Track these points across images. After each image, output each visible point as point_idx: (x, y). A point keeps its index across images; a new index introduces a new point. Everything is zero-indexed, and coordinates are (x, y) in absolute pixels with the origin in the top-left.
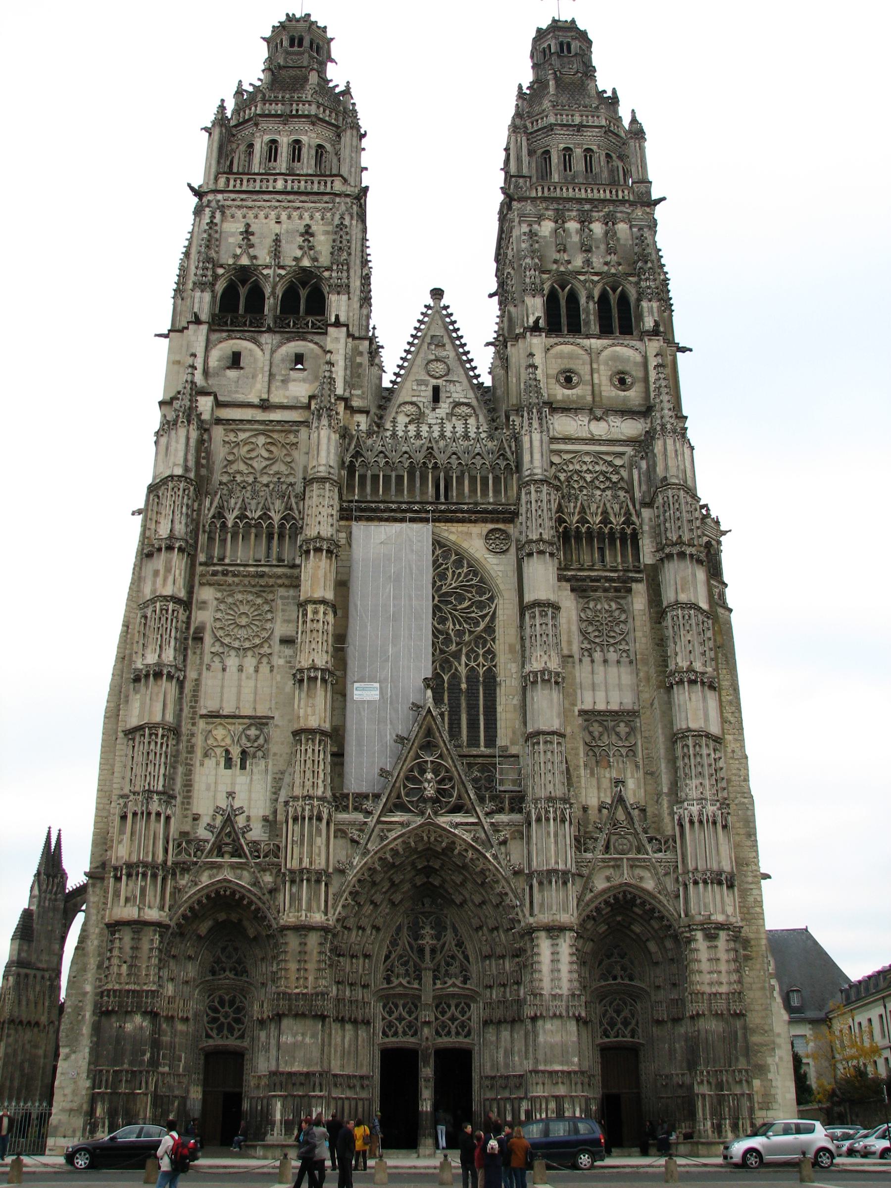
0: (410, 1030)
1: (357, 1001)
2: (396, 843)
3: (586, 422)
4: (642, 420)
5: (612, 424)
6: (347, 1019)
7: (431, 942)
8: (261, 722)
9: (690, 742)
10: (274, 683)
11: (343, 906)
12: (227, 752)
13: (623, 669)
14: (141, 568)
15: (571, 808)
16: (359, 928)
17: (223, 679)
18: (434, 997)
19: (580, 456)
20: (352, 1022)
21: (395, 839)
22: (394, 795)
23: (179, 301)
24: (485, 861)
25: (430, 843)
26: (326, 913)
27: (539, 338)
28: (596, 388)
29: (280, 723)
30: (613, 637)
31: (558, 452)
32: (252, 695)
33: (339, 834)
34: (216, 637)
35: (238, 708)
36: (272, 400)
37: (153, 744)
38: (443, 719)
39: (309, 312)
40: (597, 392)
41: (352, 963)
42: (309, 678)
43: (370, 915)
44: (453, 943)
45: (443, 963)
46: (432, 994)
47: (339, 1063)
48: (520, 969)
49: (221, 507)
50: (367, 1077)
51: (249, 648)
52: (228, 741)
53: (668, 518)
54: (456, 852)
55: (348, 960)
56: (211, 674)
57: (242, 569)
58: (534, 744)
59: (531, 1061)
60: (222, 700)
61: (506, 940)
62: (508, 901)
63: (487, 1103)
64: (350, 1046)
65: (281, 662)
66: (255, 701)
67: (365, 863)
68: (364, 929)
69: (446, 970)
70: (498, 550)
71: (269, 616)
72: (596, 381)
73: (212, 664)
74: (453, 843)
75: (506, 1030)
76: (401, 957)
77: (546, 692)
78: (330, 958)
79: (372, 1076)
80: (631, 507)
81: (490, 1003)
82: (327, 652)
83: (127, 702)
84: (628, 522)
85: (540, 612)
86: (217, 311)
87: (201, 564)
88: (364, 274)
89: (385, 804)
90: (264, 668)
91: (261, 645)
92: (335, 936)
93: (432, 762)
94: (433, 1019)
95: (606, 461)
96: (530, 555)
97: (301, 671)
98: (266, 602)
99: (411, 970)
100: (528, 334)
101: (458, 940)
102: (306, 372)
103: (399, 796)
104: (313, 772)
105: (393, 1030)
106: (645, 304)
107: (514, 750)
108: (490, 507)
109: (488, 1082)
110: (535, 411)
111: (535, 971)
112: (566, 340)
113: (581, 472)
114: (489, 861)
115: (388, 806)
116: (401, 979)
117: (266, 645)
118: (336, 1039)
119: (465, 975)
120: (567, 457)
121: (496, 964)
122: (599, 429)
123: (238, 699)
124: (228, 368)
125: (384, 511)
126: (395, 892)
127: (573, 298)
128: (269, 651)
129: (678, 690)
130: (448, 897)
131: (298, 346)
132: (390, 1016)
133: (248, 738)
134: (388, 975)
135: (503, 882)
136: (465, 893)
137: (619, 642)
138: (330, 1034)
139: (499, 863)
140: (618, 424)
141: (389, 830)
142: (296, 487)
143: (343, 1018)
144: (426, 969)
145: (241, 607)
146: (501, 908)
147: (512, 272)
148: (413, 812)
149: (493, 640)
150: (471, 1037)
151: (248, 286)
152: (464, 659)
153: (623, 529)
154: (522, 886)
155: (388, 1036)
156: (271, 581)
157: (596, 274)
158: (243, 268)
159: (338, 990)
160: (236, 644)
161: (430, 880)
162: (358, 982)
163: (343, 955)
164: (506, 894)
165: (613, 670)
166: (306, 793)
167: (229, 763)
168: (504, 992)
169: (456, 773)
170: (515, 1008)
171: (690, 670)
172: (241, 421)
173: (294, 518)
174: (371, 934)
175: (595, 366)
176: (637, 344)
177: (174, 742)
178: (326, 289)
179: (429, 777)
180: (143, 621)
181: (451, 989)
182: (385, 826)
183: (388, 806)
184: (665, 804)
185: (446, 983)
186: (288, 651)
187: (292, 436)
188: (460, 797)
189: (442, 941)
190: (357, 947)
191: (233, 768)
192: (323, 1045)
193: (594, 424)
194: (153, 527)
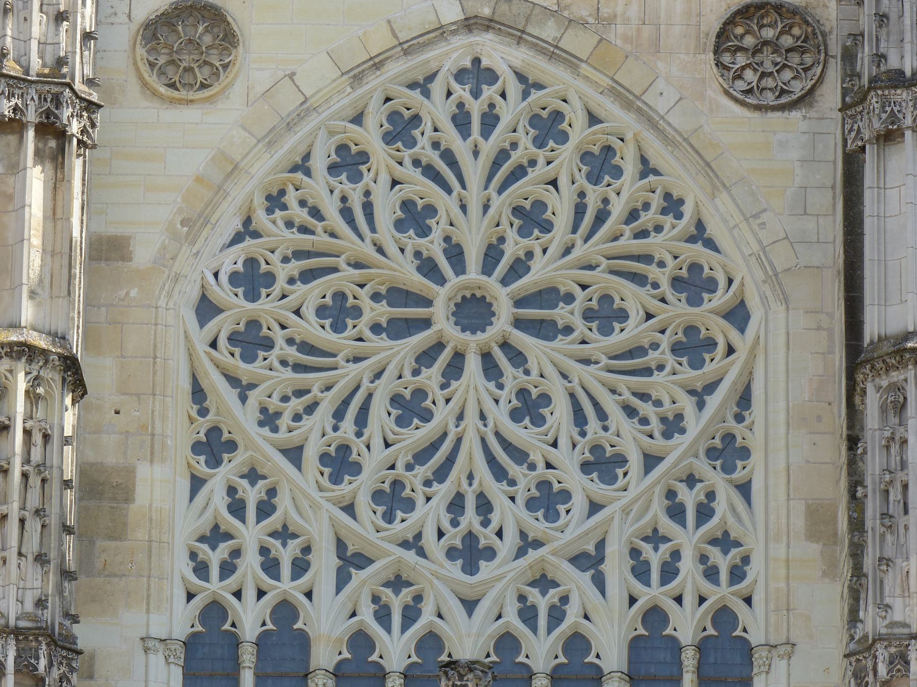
82: (41, 559)
149: (745, 489)
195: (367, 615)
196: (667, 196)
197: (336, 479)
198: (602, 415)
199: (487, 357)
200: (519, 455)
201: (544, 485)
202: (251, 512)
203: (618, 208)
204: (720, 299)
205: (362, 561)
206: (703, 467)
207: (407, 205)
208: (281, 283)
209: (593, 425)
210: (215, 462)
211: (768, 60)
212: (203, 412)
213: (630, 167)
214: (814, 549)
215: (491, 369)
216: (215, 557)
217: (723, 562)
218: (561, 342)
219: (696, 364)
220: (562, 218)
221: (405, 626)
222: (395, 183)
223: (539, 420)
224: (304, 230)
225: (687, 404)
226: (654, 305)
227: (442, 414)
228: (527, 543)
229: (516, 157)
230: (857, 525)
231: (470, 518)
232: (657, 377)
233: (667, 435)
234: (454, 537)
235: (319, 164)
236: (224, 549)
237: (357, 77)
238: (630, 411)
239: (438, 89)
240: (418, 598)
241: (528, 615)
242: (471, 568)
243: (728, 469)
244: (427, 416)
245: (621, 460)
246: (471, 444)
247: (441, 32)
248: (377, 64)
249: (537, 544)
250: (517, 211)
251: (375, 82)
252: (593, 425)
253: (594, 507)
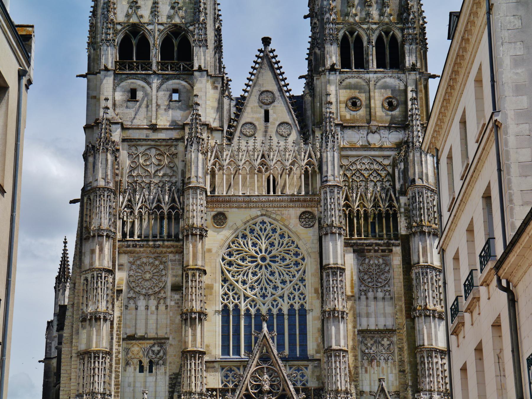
3: (365, 135)
4: (403, 132)
5: (382, 136)
8: (161, 341)
9: (425, 355)
10: (168, 318)
12: (141, 362)
13: (386, 303)
14: (81, 246)
15: (351, 396)
17: (136, 315)
19: (361, 159)
22: (244, 389)
23: (92, 51)
27: (335, 75)
28: (372, 111)
29: (173, 343)
30: (380, 282)
31: (347, 157)
32: (155, 325)
34: (130, 288)
35: (146, 333)
36: (158, 123)
37: (97, 363)
38: (273, 342)
39: (180, 59)
40: (373, 114)
42: (191, 317)
49: (129, 201)
51: (152, 294)
52: (141, 354)
53: (415, 207)
56: (128, 311)
57: (145, 243)
58: (328, 357)
60: (136, 329)
65: (173, 303)
66: (157, 328)
70: (307, 226)
71: (164, 273)
72: (372, 105)
73: (129, 305)
77: (336, 323)
80: (393, 196)
83: (78, 333)
84: (391, 206)
85: (333, 272)
86: (118, 60)
87: (119, 241)
88: (216, 27)
89: (239, 395)
90: (162, 307)
91: (159, 292)
93: (267, 368)
95: (378, 162)
96: (326, 234)
97: (186, 314)
98: (161, 263)
100: (327, 73)
102: (180, 103)
103: (247, 390)
104: (195, 377)
106: (407, 47)
107: (318, 356)
108: (302, 198)
110: (330, 136)
112: (353, 75)
113: (361, 170)
115: (240, 396)
117: (162, 292)
120: (352, 160)
122: (374, 139)
123: (146, 328)
124: (128, 101)
125: (234, 202)
127: (359, 39)
128: (164, 296)
129: (418, 321)
131: (175, 84)
133: (153, 351)
137: (385, 286)
140: (387, 135)
142: (177, 184)
145: (146, 267)
147: (317, 22)
149: (305, 286)
151: (138, 37)
152: (286, 298)
153: (388, 210)
156: (164, 250)
157: (375, 23)
158: (134, 25)
160: (144, 291)
165: (380, 304)
166: (190, 390)
167: (141, 370)
169: (281, 375)
171: (426, 309)
172: (139, 140)
173: (178, 209)
175: (372, 94)
176: (402, 76)
177: (109, 360)
178: (191, 39)
179: (265, 378)
180: (85, 282)
183: (240, 396)
184: (410, 392)
186: (177, 297)
187: (173, 149)
188: (284, 390)
191: (145, 372)
193: (370, 135)
194: (88, 220)
195: (249, 306)
196: (292, 241)
197: (243, 285)
198: (283, 275)
199: (266, 266)
200: (271, 281)
201: (275, 286)
202: (231, 291)
203: (285, 243)
204: (301, 257)
205: (248, 298)
206: (298, 282)
207: (253, 243)
208: (235, 255)
209: (282, 276)
210: (225, 283)
211: (307, 220)
212: (223, 275)
213: (286, 236)
214: (316, 295)
215: (266, 268)
216: (225, 298)
217: (302, 297)
218: (277, 264)
219: (297, 267)
220: (276, 245)
221: (254, 307)
222: (251, 239)
223: (274, 276)
224: (238, 247)
225: (296, 273)
226: (291, 258)
227: (259, 275)
228: (272, 295)
229: (269, 235)
230: (322, 293)
231: (264, 291)
232: (291, 269)
233: (293, 278)
234: (261, 294)
235: (240, 236)
236: (227, 296)
237: (245, 224)
238: (287, 274)
239: (257, 225)
240: (256, 303)
241: (273, 305)
242: (264, 299)
243: (302, 283)
244: (257, 275)
245: (286, 282)
246: (264, 280)
247: (258, 216)
248: (248, 221)
249: (274, 295)
250: (270, 244)
251: (248, 224)
252: (282, 276)
253: (282, 289)
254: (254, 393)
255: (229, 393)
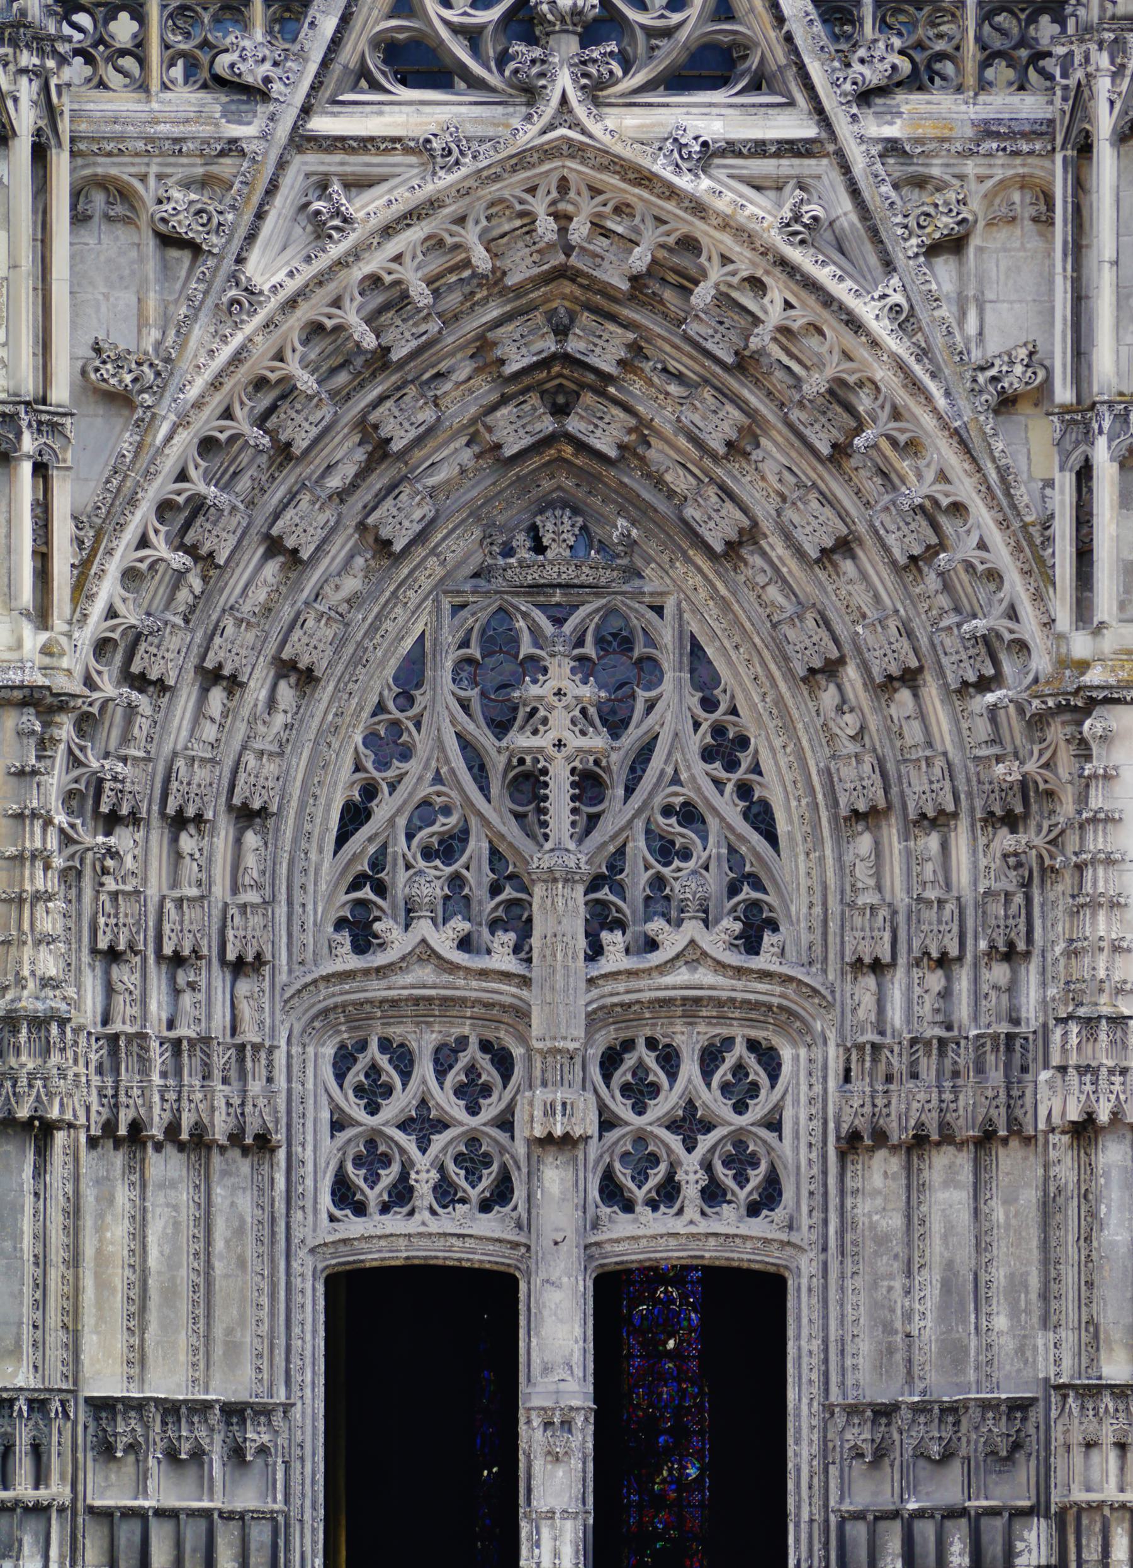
0: (473, 1177)
1: (206, 1040)
2: (393, 247)
6: (156, 1131)
7: (575, 742)
11: (131, 576)
16: (211, 677)
18: (593, 1021)
20: (181, 1147)
21: (387, 231)
24: (849, 340)
25: (568, 250)
26: (42, 616)
33: (99, 199)
41: (177, 856)
43: (268, 610)
44: (695, 742)
45: (638, 845)
46: (582, 1000)
47: (119, 1343)
48: (1026, 885)
50: (264, 1412)
54: (703, 295)
55: (158, 836)
59: (1068, 1337)
61: (961, 745)
62: (967, 549)
63: (858, 1532)
64: (171, 1263)
67: (237, 359)
68: (234, 684)
69: (659, 882)
74: (689, 245)
75: (948, 1183)
76: (426, 811)
78: (66, 839)
79: (287, 1408)
81: (876, 1048)
89: (336, 43)
92: (86, 723)
94: (586, 1123)
99: (478, 879)
101: (718, 731)
105: (389, 1176)
109: (861, 1435)
111: (1094, 905)
114: (875, 344)
115: (348, 56)
116: (424, 928)
118: (100, 1230)
119: (755, 905)
121: (908, 852)
126: (391, 489)
130: (662, 506)
132: (373, 1109)
134: (361, 903)
135: (945, 452)
136: (746, 489)
138: (74, 1212)
139: (923, 353)
141: (357, 184)
143: (136, 1127)
144: (551, 878)
146: (932, 581)
148: (476, 83)
150: (779, 1214)
154: (1040, 473)
155: (360, 1210)
159: (109, 990)
161: (574, 425)
162: (208, 947)
163: (134, 819)
164: (958, 509)
168: (946, 994)
170: (996, 1077)
174: (272, 703)
181: (682, 976)
182: (332, 163)
185: (652, 945)
189: (632, 737)
190: (201, 774)
192: (41, 1261)
254: (472, 35)
255: (246, 26)
